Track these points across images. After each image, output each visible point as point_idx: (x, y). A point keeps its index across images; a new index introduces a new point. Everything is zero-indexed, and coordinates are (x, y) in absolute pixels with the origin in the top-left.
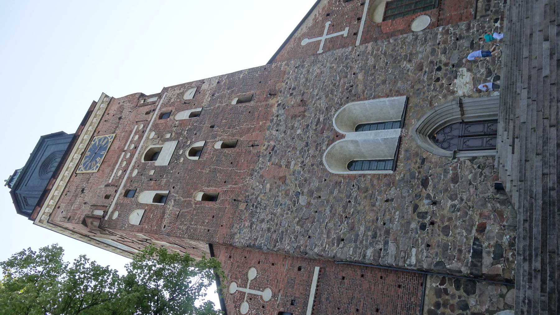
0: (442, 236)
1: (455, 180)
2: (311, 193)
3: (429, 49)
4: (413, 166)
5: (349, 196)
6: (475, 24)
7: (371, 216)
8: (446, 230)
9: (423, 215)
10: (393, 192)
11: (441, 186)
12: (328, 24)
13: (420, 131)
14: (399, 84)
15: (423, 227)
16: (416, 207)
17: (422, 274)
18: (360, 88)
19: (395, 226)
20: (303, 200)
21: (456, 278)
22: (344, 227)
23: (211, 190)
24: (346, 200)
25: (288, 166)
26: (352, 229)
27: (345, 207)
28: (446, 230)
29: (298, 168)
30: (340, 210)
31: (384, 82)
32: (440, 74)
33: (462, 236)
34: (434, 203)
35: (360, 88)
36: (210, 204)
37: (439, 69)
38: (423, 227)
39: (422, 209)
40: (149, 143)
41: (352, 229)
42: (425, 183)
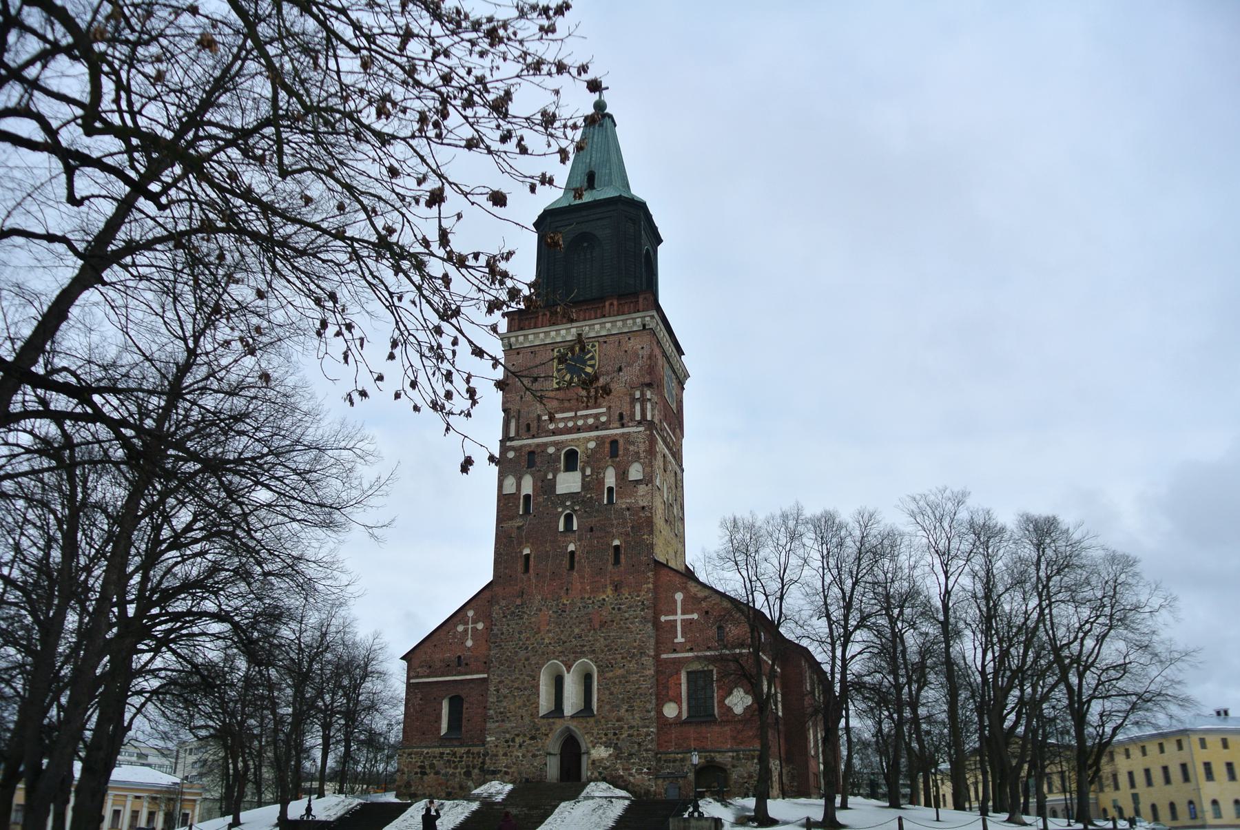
0: (501, 753)
1: (534, 756)
2: (527, 659)
3: (634, 724)
4: (543, 730)
5: (525, 689)
6: (650, 754)
7: (512, 707)
8: (505, 754)
9: (513, 740)
10: (527, 720)
11: (530, 748)
12: (695, 616)
13: (568, 728)
14: (607, 707)
15: (507, 741)
16: (518, 735)
17: (484, 743)
18: (610, 675)
19: (508, 725)
20: (522, 654)
21: (483, 763)
22: (505, 691)
23: (532, 559)
24: (522, 687)
25: (549, 631)
26: (505, 697)
27: (518, 688)
28: (505, 754)
29: (547, 641)
30: (516, 685)
31: (611, 694)
32: (610, 736)
33: (503, 762)
34: (520, 746)
35: (610, 675)
36: (520, 567)
37: (615, 734)
38: (507, 741)
39: (517, 740)
40: (583, 448)
41: (505, 697)
42: (533, 738)
